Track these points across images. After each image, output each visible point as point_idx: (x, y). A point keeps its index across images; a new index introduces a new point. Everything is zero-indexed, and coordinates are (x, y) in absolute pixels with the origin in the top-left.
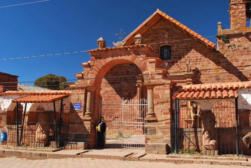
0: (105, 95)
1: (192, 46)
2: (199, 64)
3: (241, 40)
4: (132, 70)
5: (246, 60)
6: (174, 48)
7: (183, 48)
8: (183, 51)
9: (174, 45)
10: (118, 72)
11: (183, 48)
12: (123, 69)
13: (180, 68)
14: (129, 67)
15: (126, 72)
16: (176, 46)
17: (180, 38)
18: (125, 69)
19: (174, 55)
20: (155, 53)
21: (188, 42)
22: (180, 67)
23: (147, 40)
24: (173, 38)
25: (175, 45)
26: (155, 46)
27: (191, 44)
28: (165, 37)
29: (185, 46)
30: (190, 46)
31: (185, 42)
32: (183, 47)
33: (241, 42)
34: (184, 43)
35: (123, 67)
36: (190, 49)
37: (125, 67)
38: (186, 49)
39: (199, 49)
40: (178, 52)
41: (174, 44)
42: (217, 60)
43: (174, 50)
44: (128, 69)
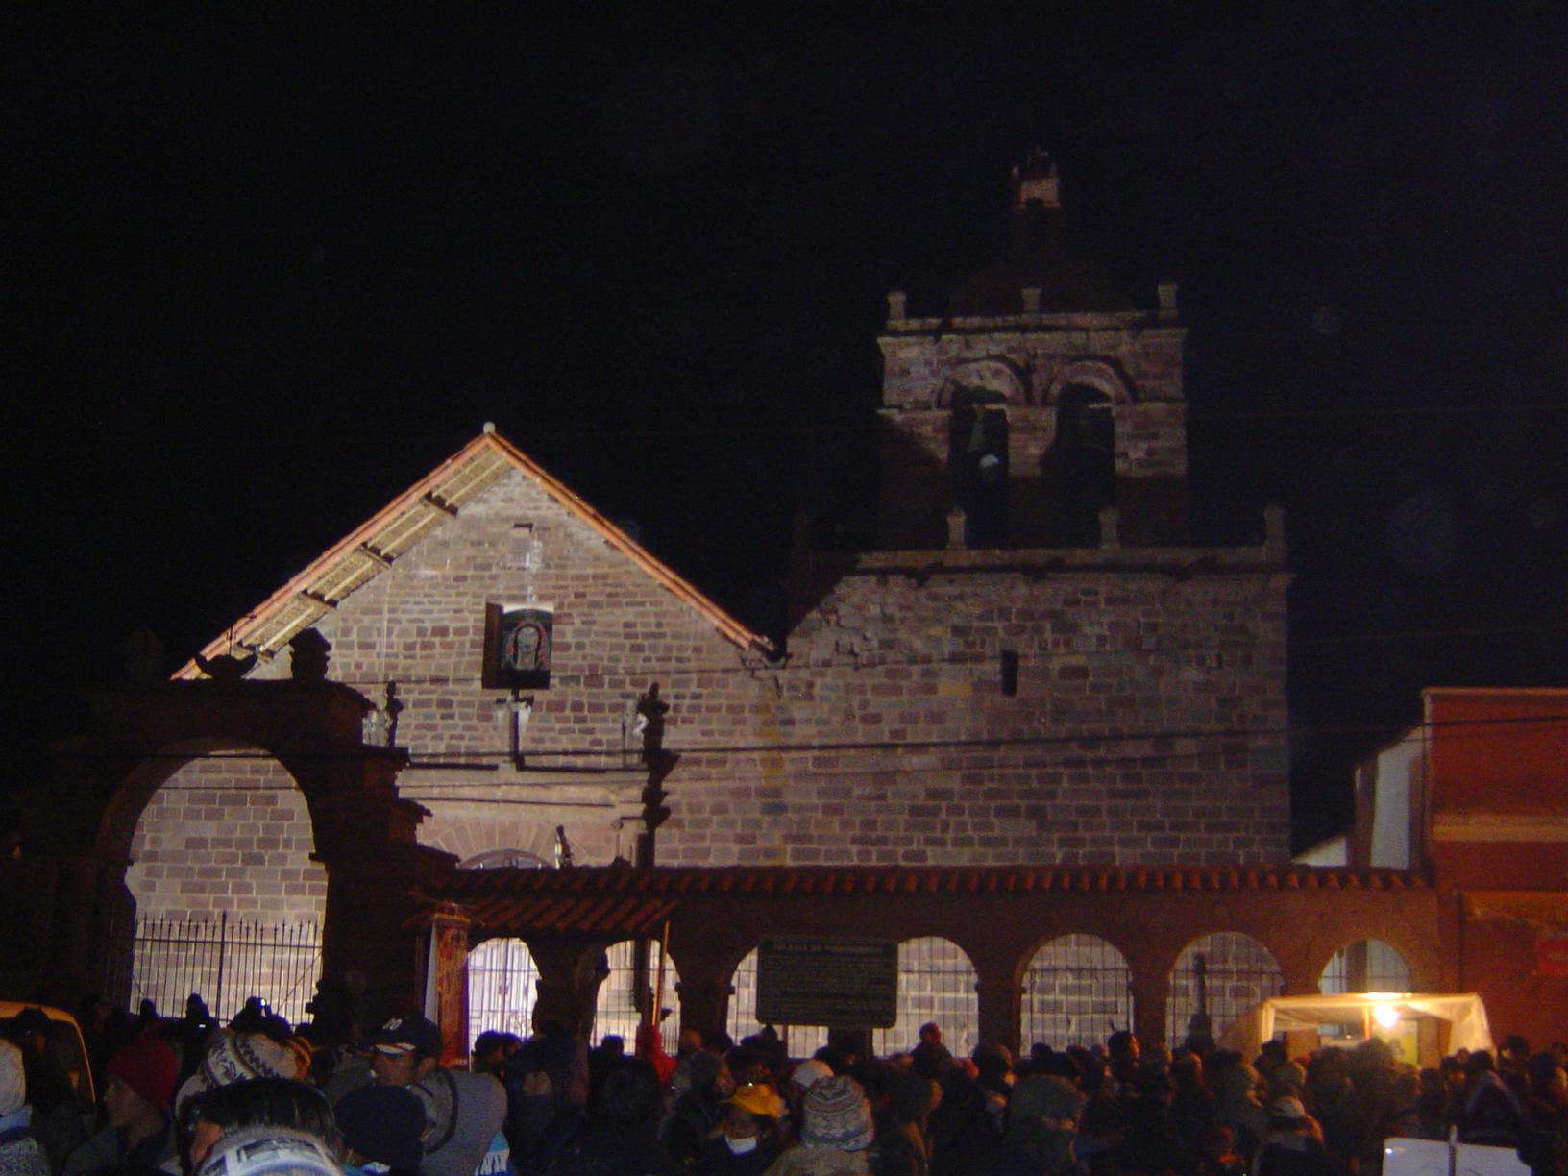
2: (691, 721)
3: (898, 614)
5: (913, 719)
6: (568, 630)
7: (611, 635)
8: (614, 647)
9: (570, 615)
11: (611, 635)
16: (577, 621)
17: (604, 577)
20: (467, 649)
21: (642, 604)
22: (591, 731)
24: (565, 577)
25: (574, 612)
26: (470, 612)
27: (656, 614)
28: (524, 569)
29: (627, 625)
30: (648, 625)
31: (624, 600)
32: (611, 624)
33: (898, 622)
34: (617, 605)
36: (646, 643)
38: (627, 636)
39: (691, 643)
40: (588, 651)
41: (570, 606)
42: (781, 708)
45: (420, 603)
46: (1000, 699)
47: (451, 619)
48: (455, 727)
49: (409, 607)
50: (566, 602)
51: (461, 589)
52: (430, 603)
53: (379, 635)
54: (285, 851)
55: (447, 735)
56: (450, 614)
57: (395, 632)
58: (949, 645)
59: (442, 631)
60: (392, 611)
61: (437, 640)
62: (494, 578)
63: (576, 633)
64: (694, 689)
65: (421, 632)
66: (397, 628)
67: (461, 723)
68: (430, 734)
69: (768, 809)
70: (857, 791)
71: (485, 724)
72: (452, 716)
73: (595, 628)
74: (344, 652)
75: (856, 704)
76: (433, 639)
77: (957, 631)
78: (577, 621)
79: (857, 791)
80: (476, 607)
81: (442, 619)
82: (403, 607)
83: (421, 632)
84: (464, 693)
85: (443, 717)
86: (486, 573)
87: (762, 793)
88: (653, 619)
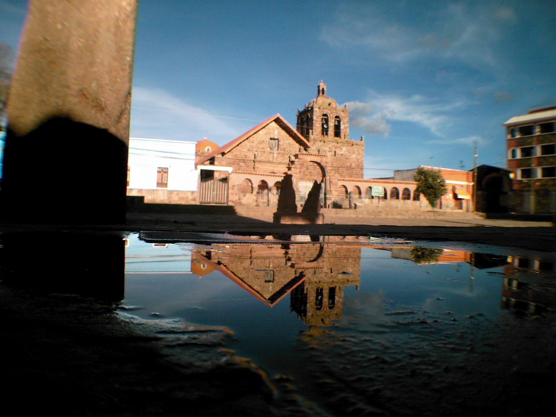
14: (247, 152)
46: (333, 157)
58: (328, 150)
65: (261, 141)
69: (306, 169)
77: (330, 148)
83: (261, 141)
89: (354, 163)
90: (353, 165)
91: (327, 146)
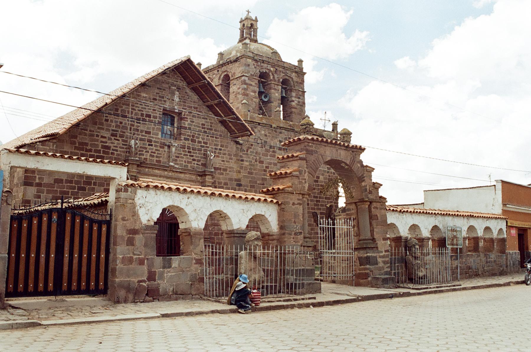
0: (55, 189)
1: (211, 126)
3: (268, 134)
4: (114, 146)
5: (270, 164)
6: (186, 123)
9: (187, 118)
10: (87, 144)
12: (97, 141)
13: (192, 158)
14: (110, 139)
15: (103, 147)
16: (189, 120)
17: (197, 108)
18: (102, 142)
19: (185, 135)
21: (207, 119)
22: (193, 156)
23: (145, 95)
24: (185, 106)
25: (188, 117)
27: (211, 123)
29: (203, 124)
30: (208, 126)
31: (202, 117)
34: (200, 118)
35: (97, 136)
37: (102, 137)
38: (203, 128)
41: (187, 115)
43: (186, 126)
44: (106, 143)
45: (141, 105)
47: (152, 112)
48: (152, 149)
49: (138, 105)
50: (186, 114)
51: (155, 103)
52: (145, 105)
53: (128, 113)
54: (94, 187)
55: (150, 151)
56: (152, 111)
57: (134, 113)
59: (149, 116)
60: (132, 105)
61: (147, 118)
62: (165, 101)
63: (189, 124)
64: (219, 147)
66: (134, 112)
67: (155, 148)
68: (145, 150)
70: (258, 182)
71: (162, 149)
72: (152, 145)
73: (194, 124)
74: (116, 117)
75: (258, 158)
76: (146, 118)
78: (189, 120)
79: (258, 182)
80: (160, 110)
81: (149, 112)
82: (137, 105)
84: (156, 138)
85: (149, 145)
86: (163, 99)
87: (236, 180)
88: (209, 124)
89: (323, 175)
90: (321, 178)
91: (277, 138)
